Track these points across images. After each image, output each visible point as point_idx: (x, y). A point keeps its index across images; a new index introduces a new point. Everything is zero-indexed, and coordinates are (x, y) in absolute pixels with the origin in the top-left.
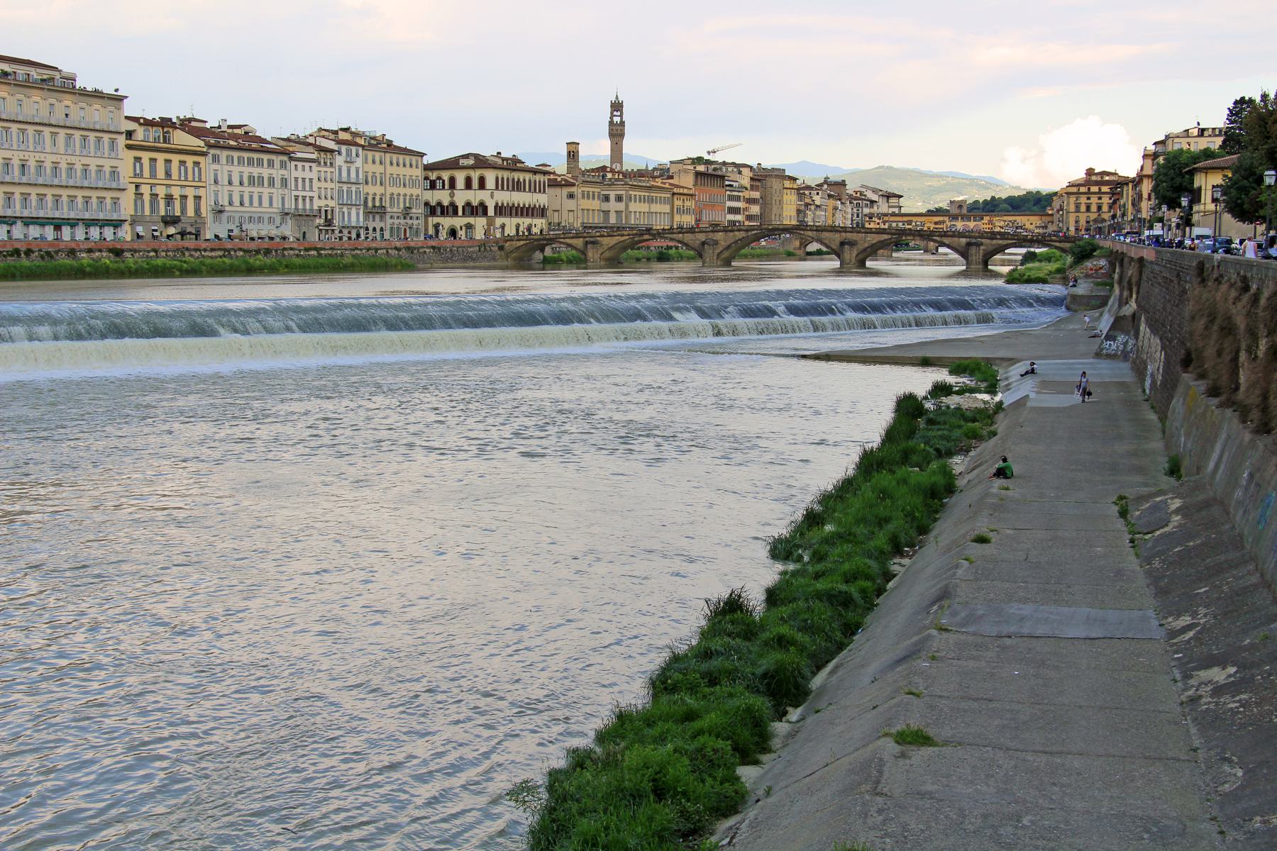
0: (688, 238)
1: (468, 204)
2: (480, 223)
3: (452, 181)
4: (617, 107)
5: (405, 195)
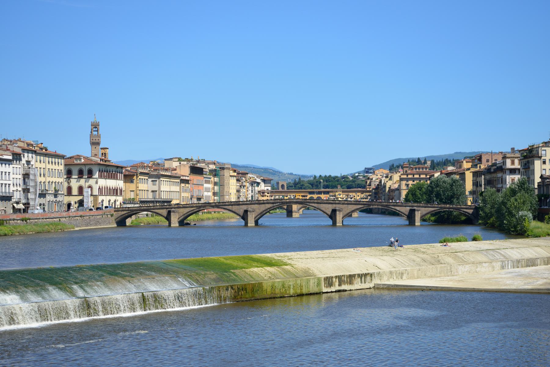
4: (95, 126)
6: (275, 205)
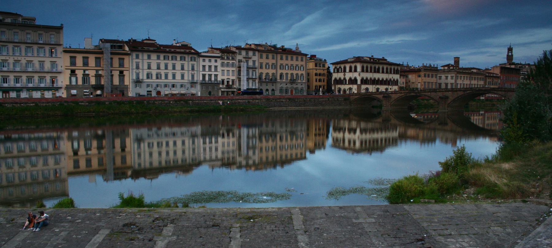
0: (433, 95)
1: (350, 79)
2: (354, 88)
3: (345, 68)
5: (287, 74)
6: (466, 92)
